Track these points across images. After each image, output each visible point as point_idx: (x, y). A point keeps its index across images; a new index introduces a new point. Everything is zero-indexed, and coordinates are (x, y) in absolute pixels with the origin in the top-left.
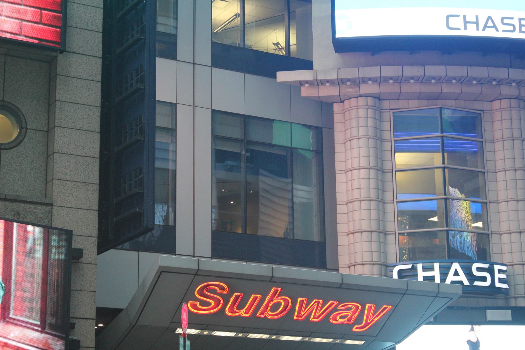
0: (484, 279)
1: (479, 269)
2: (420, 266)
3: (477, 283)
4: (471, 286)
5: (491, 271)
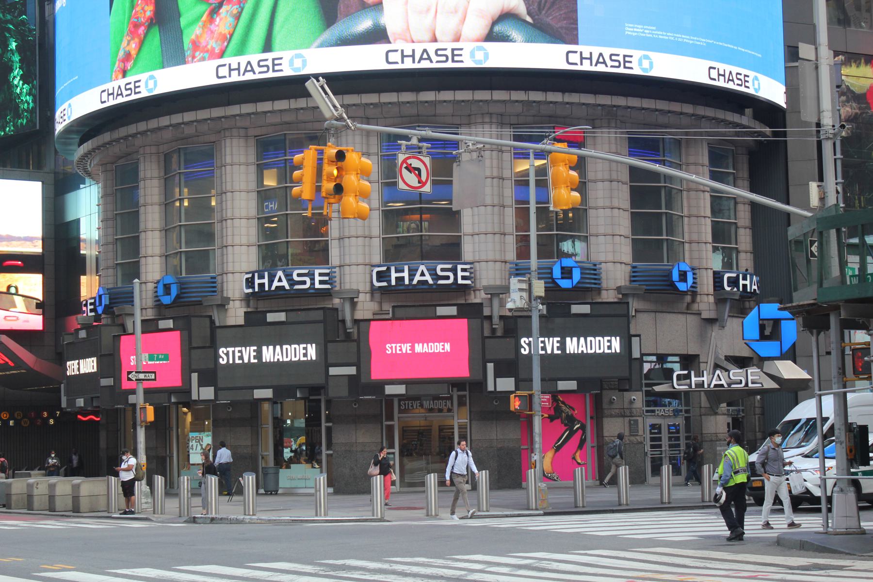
0: (448, 278)
1: (442, 270)
2: (393, 269)
3: (441, 282)
4: (435, 284)
5: (454, 271)
